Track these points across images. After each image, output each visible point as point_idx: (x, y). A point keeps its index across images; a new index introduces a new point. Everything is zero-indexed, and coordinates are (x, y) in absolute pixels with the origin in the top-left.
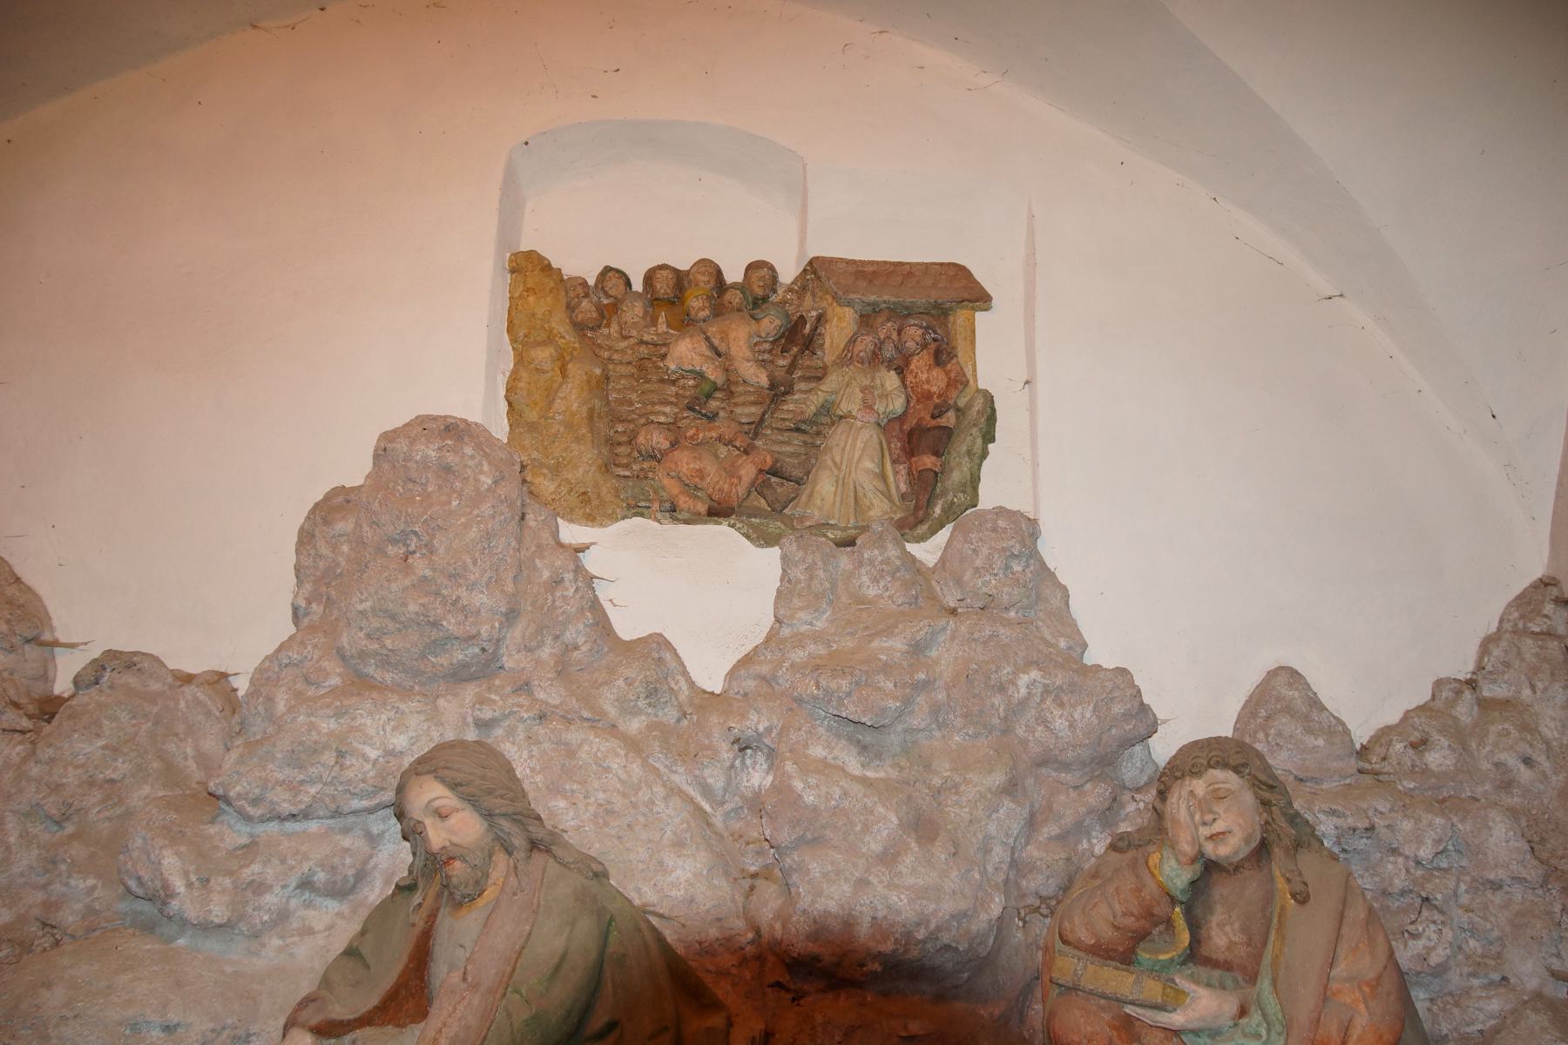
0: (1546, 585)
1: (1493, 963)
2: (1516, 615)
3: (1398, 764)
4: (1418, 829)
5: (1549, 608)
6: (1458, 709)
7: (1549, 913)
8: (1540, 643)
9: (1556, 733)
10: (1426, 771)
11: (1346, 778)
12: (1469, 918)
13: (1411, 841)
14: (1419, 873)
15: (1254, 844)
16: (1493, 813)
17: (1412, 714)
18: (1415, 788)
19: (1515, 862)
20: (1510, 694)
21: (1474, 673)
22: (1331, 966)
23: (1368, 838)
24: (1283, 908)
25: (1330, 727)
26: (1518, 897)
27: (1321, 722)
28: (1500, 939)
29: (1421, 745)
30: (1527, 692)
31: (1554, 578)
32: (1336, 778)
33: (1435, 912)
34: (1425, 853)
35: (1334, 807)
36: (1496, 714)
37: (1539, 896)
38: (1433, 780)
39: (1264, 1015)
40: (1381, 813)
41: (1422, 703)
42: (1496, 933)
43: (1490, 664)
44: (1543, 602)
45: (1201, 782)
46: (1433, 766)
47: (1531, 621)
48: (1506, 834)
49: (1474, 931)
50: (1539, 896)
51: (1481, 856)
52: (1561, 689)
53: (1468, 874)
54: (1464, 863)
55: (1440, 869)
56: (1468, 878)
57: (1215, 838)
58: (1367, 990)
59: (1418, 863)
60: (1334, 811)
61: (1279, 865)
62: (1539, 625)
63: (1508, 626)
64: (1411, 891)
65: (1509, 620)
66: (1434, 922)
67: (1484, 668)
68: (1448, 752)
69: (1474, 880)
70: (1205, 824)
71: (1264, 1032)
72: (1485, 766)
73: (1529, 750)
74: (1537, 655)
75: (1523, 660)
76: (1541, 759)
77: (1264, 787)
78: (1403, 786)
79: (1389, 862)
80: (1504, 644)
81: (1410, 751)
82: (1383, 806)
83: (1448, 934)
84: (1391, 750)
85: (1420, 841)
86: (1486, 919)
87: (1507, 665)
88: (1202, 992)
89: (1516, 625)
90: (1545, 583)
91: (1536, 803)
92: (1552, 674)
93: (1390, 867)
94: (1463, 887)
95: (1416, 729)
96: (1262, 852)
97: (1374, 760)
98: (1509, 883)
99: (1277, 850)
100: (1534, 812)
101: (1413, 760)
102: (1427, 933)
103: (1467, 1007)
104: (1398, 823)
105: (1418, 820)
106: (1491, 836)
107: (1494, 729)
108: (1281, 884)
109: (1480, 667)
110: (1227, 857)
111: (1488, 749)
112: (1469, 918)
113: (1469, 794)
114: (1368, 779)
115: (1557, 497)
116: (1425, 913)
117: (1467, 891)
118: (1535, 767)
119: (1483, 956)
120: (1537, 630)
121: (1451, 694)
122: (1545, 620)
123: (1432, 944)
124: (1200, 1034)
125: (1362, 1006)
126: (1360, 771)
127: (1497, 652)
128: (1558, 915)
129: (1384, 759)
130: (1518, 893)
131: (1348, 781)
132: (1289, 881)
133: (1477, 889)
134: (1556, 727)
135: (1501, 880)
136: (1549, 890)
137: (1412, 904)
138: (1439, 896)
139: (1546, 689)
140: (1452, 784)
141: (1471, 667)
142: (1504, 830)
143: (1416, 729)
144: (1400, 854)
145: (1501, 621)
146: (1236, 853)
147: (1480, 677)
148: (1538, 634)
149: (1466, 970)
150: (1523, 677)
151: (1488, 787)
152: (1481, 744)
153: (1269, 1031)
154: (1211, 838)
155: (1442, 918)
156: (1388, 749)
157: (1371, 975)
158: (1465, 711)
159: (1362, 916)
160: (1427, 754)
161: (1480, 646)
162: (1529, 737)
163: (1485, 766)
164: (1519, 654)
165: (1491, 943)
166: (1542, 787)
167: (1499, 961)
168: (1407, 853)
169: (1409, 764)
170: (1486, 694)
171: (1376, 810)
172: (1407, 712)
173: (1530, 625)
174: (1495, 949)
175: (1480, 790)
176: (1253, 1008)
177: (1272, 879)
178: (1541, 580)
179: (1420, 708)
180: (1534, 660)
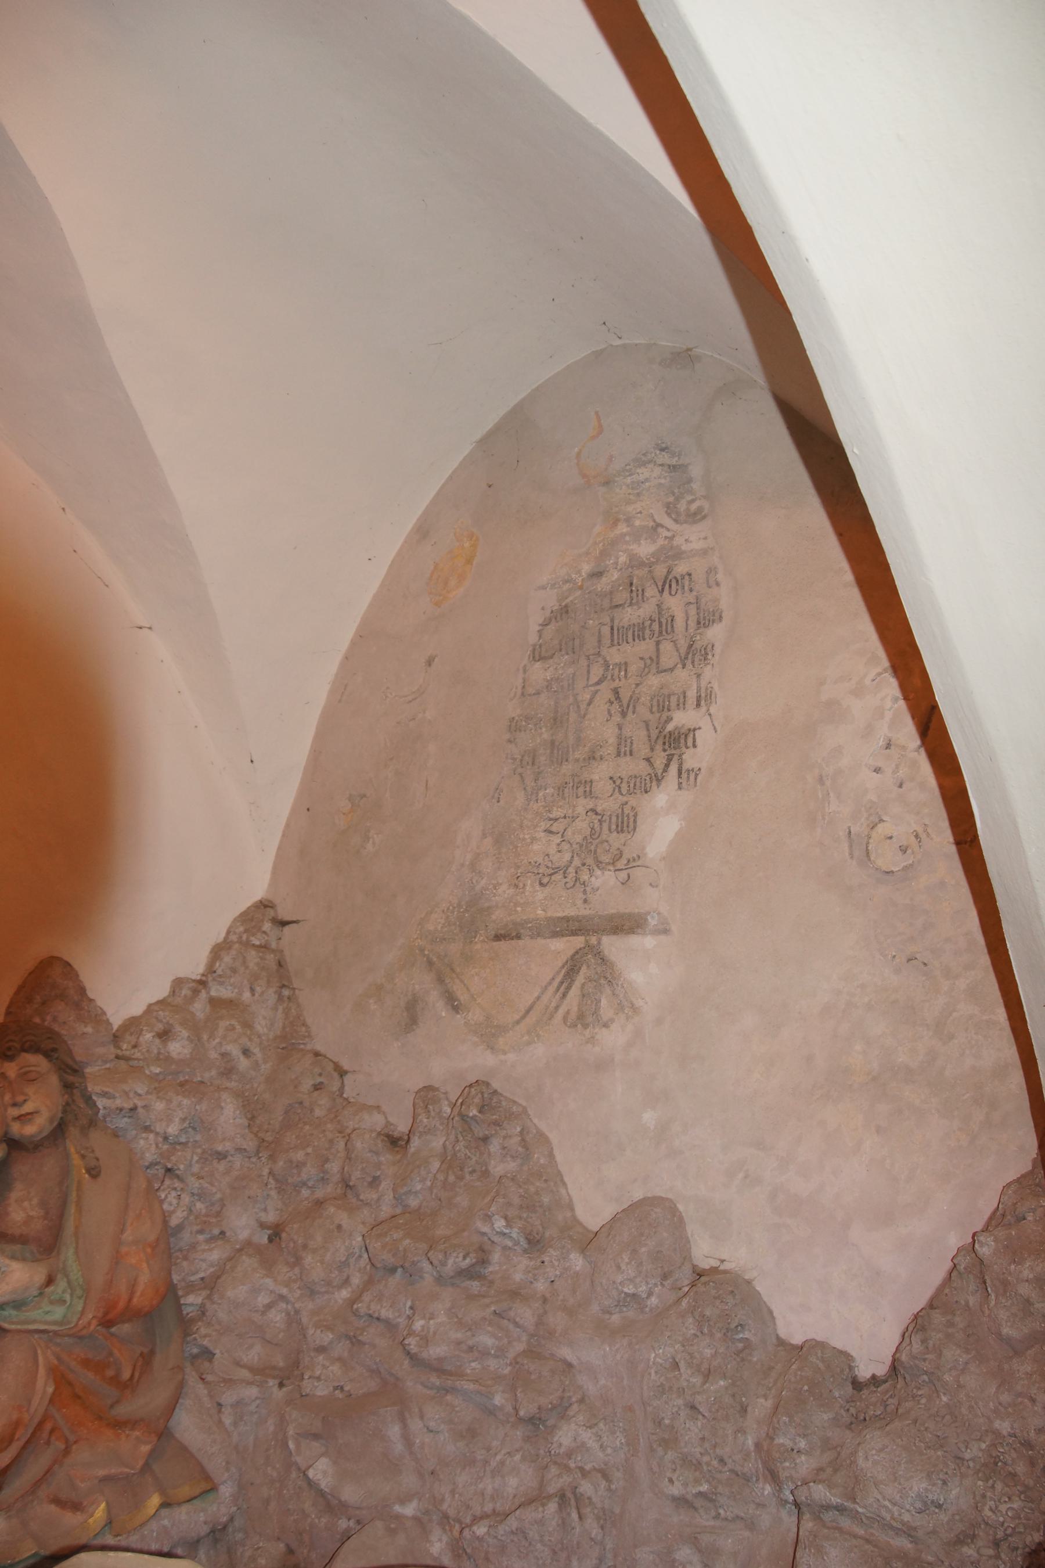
0: (266, 906)
1: (214, 1220)
2: (242, 929)
3: (148, 1051)
4: (169, 1109)
5: (267, 926)
6: (196, 1005)
7: (260, 1176)
8: (261, 954)
9: (265, 1029)
10: (168, 1059)
11: (106, 1062)
12: (200, 1184)
13: (162, 1120)
14: (166, 1147)
15: (55, 1124)
16: (225, 1096)
17: (156, 1008)
18: (160, 1073)
19: (238, 1136)
20: (234, 995)
21: (203, 975)
22: (122, 1231)
23: (130, 1117)
24: (80, 1183)
25: (96, 1015)
26: (237, 1165)
27: (89, 1011)
28: (221, 1200)
29: (165, 1035)
30: (247, 995)
31: (271, 902)
32: (99, 1062)
33: (176, 1180)
34: (173, 1130)
35: (106, 1089)
36: (224, 1011)
37: (253, 1163)
38: (173, 1067)
39: (69, 1282)
40: (140, 1095)
41: (161, 998)
42: (218, 1196)
43: (221, 969)
44: (262, 921)
45: (13, 1064)
46: (174, 1055)
47: (253, 935)
48: (234, 1112)
49: (201, 1196)
50: (253, 1163)
51: (212, 1131)
52: (273, 995)
53: (200, 1147)
54: (198, 1137)
55: (180, 1144)
56: (199, 1151)
57: (22, 1118)
58: (149, 1250)
59: (166, 1138)
60: (106, 1093)
61: (72, 1145)
62: (259, 939)
63: (234, 938)
64: (157, 1164)
65: (235, 933)
66: (175, 1189)
67: (215, 972)
68: (187, 1043)
69: (204, 1152)
70: (15, 1105)
71: (67, 1297)
72: (213, 1055)
73: (249, 1043)
74: (258, 964)
75: (247, 968)
76: (256, 1051)
77: (69, 1071)
78: (151, 1072)
79: (142, 1138)
80: (233, 952)
81: (157, 1041)
82: (141, 1089)
83: (186, 1199)
84: (141, 1039)
85: (170, 1120)
86: (212, 1185)
87: (234, 971)
88: (15, 1265)
89: (241, 937)
90: (264, 905)
91: (248, 1087)
92: (268, 982)
93: (142, 1142)
94: (196, 1158)
95: (161, 1021)
96: (59, 1131)
97: (125, 1047)
98: (233, 1153)
99: (72, 1129)
100: (247, 1094)
101: (159, 1048)
102: (169, 1199)
103: (195, 1259)
104: (153, 1103)
105: (170, 1101)
106: (222, 1114)
107: (223, 1024)
108: (76, 1160)
109: (210, 970)
110: (32, 1136)
111: (217, 1040)
112: (200, 1184)
113: (199, 1079)
114: (123, 1065)
115: (283, 836)
116: (167, 1182)
117: (197, 1162)
118: (250, 1056)
119: (207, 1215)
120: (257, 943)
121: (189, 993)
122: (264, 935)
123: (172, 1208)
124: (4, 1306)
125: (145, 1265)
126: (117, 1057)
127: (227, 959)
128: (266, 1178)
129: (135, 1047)
130: (238, 1161)
131: (108, 1066)
132: (83, 1157)
133: (206, 1159)
134: (266, 1024)
135: (227, 1151)
136: (260, 1158)
137: (156, 1175)
138: (182, 1167)
139: (263, 993)
140: (188, 1070)
141: (201, 969)
142: (232, 1110)
143: (161, 1021)
144: (151, 1131)
145: (228, 932)
146: (40, 1132)
147: (210, 979)
148: (258, 946)
149: (196, 1228)
150: (246, 982)
151: (214, 1073)
152: (212, 1036)
153: (72, 1295)
154: (19, 1118)
155: (181, 1186)
156: (138, 1038)
157: (152, 1238)
158: (200, 1008)
159: (144, 1186)
160: (169, 1044)
161: (211, 952)
162: (249, 1032)
163: (213, 1055)
164: (244, 962)
165: (213, 1204)
166: (253, 1073)
167: (219, 1219)
168: (158, 1130)
169: (156, 1051)
170: (213, 993)
171: (136, 1093)
172: (150, 1005)
173: (252, 938)
174: (217, 1208)
175: (207, 1075)
176: (59, 1276)
177: (67, 1156)
178: (261, 902)
179: (159, 1002)
180: (256, 968)
